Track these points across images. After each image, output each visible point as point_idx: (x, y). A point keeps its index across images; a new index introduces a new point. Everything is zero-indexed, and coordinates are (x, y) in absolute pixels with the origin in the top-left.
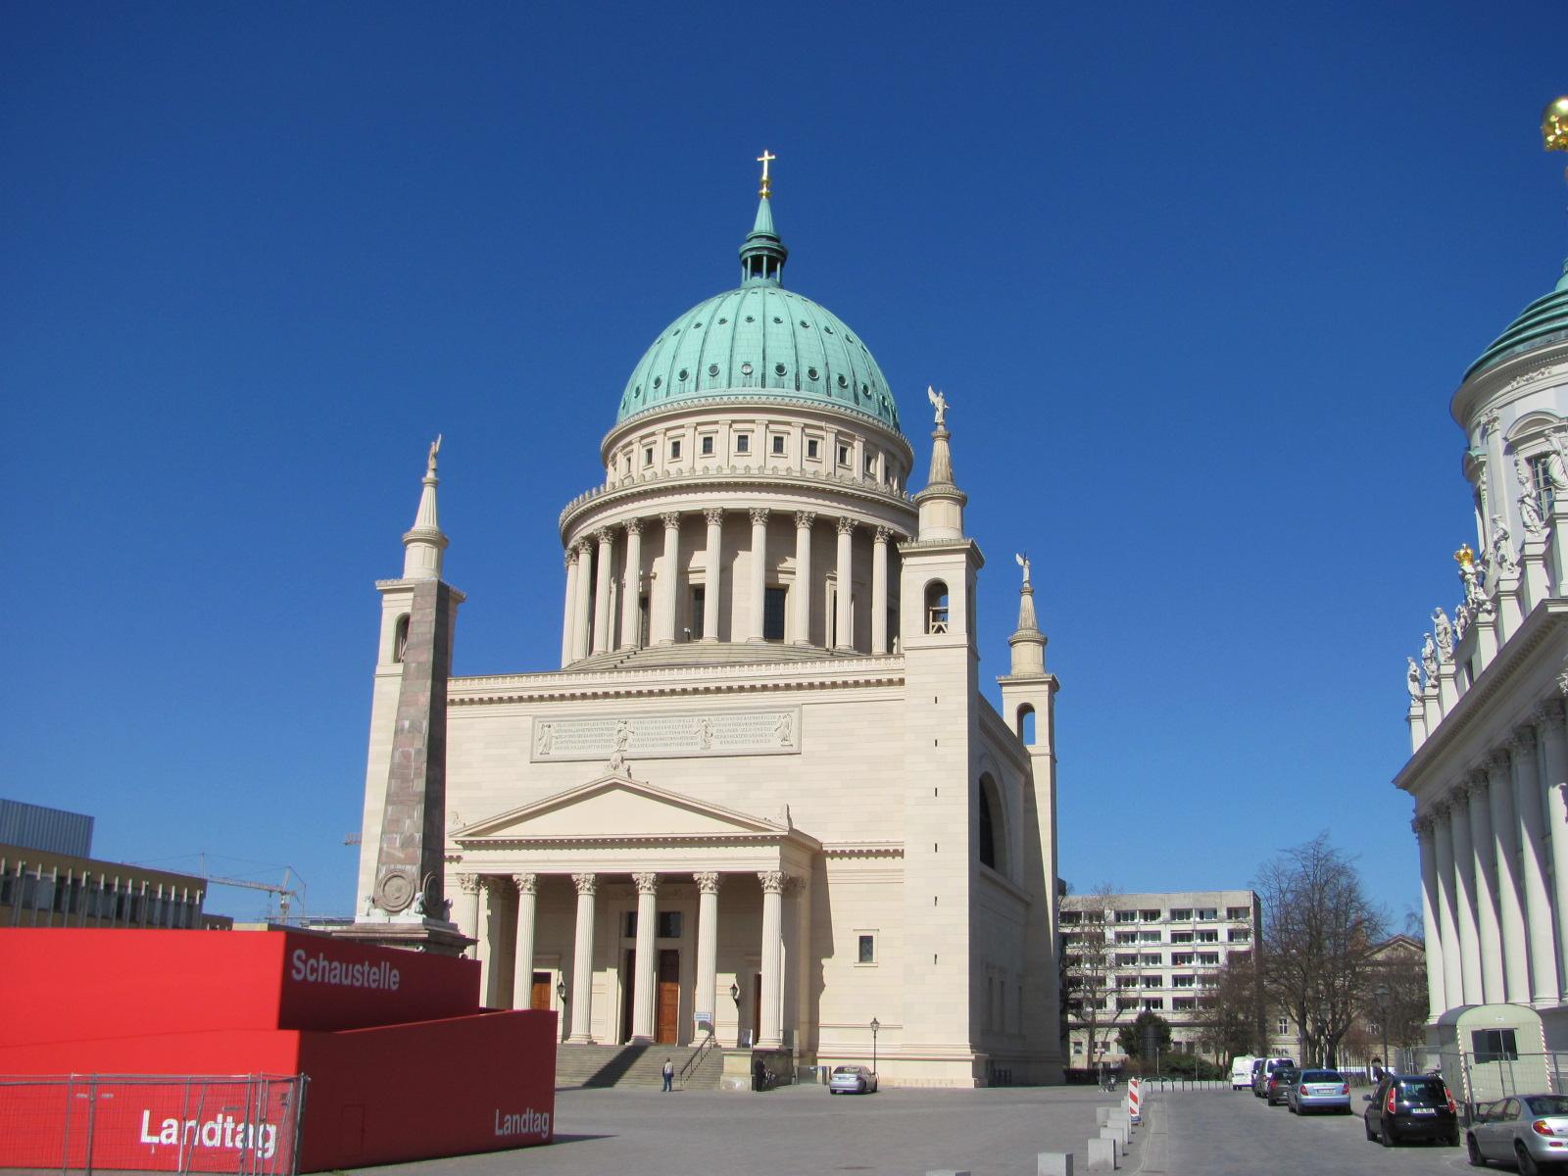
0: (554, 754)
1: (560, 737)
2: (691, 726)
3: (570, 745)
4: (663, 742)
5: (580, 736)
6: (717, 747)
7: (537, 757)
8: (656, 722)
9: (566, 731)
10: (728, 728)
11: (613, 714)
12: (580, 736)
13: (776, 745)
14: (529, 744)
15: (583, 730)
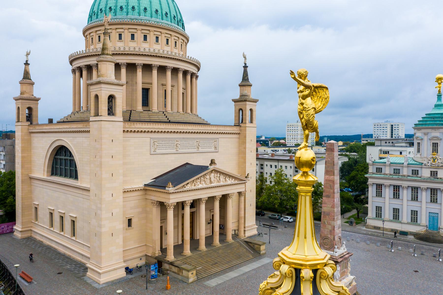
0: (158, 151)
1: (159, 145)
2: (194, 143)
3: (162, 148)
4: (188, 148)
5: (165, 145)
6: (201, 150)
7: (152, 153)
8: (185, 141)
9: (160, 143)
10: (203, 144)
11: (175, 138)
12: (165, 145)
13: (213, 150)
14: (149, 148)
15: (166, 143)
